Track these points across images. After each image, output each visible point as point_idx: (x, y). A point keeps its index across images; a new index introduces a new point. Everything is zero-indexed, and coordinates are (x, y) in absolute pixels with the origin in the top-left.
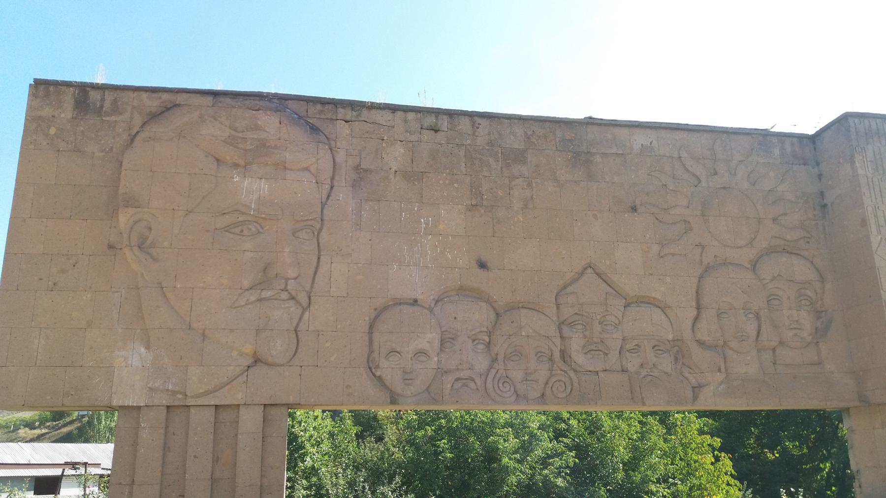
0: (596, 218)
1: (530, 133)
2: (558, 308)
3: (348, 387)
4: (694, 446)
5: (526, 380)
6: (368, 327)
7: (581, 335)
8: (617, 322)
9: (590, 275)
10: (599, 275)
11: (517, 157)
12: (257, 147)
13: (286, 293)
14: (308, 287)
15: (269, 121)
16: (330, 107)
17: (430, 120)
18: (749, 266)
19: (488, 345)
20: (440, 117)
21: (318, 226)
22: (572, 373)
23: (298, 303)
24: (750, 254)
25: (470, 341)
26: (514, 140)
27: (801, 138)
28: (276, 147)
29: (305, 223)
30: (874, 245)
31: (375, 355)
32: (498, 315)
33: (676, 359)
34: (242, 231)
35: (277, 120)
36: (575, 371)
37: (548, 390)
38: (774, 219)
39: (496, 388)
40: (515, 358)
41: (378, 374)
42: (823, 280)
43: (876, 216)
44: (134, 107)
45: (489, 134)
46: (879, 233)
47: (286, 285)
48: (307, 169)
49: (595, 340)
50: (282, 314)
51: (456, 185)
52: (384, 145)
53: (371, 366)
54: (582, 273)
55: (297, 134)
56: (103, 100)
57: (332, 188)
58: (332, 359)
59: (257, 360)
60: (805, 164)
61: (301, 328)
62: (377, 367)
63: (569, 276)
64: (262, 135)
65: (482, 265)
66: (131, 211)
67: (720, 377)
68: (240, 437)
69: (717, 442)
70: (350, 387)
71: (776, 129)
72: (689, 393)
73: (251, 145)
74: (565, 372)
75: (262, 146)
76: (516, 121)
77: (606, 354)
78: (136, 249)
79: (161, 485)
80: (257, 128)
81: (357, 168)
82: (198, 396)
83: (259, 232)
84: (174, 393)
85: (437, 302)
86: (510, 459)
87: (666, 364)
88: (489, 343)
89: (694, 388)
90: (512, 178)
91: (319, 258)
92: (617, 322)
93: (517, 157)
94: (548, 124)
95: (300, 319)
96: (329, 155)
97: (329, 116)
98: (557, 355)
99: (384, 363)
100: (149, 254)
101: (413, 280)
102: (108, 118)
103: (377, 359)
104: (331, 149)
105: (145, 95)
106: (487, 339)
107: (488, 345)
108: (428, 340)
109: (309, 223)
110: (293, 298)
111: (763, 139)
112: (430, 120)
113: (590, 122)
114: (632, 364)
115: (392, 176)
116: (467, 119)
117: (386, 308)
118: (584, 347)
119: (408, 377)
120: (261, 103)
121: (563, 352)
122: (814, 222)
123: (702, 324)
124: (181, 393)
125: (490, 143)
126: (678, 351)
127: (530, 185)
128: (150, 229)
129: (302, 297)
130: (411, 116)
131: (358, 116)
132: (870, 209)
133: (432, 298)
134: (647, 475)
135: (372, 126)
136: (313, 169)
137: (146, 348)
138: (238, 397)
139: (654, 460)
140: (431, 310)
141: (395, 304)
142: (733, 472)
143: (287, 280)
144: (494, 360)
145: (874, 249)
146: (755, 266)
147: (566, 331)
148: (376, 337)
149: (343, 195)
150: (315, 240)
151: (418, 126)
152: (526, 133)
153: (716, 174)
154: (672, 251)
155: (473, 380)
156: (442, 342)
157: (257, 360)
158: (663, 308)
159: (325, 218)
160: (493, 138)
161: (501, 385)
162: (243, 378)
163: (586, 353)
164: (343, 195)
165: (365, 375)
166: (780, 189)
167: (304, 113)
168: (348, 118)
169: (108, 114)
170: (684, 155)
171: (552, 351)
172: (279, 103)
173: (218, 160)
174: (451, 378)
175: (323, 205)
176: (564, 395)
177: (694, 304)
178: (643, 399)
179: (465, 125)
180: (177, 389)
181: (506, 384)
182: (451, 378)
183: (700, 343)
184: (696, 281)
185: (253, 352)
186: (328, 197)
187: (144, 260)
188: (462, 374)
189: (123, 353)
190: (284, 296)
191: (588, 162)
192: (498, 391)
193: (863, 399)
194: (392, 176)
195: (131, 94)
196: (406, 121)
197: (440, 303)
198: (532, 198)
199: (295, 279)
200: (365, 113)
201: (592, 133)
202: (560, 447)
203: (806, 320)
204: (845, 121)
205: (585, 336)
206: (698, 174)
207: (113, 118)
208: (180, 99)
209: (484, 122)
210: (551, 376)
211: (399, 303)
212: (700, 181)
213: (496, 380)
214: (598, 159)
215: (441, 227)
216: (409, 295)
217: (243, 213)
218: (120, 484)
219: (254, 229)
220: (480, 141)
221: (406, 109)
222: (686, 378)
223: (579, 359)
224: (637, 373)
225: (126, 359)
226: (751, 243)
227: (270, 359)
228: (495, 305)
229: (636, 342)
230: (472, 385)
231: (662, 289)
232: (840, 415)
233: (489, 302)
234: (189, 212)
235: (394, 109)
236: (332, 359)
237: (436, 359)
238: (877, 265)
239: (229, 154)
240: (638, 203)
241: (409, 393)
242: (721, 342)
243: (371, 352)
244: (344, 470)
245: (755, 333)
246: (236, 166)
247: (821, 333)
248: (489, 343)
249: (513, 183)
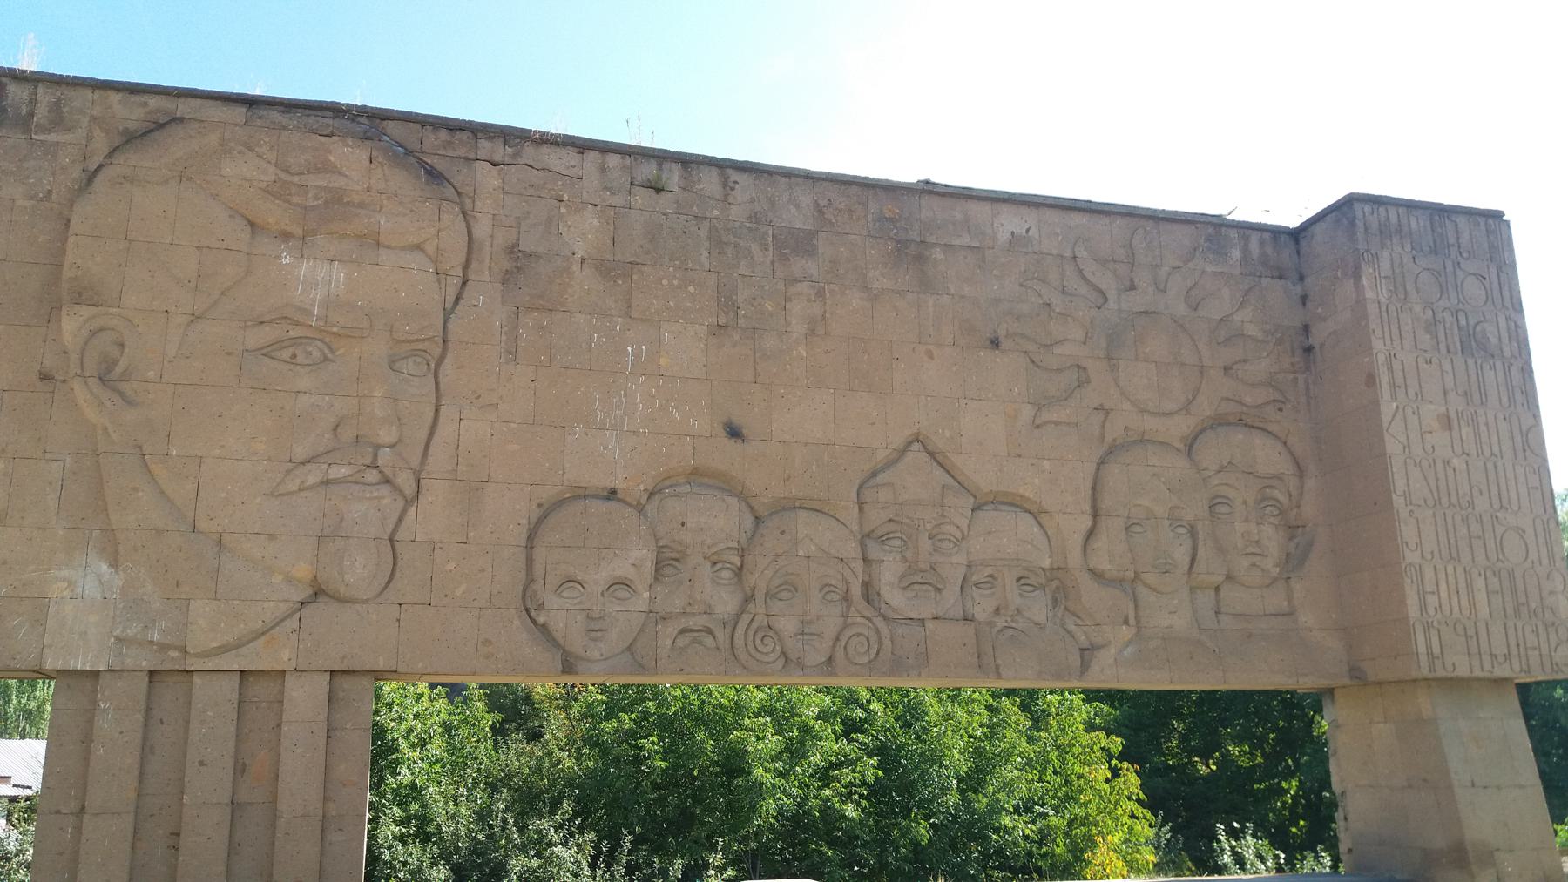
0: (931, 357)
1: (823, 203)
2: (861, 510)
3: (487, 642)
4: (1077, 750)
5: (803, 634)
6: (525, 536)
7: (898, 557)
8: (959, 535)
9: (916, 455)
10: (931, 454)
11: (802, 243)
12: (326, 202)
13: (375, 472)
14: (415, 463)
15: (351, 159)
16: (465, 136)
17: (648, 170)
18: (1181, 446)
19: (739, 571)
20: (667, 165)
21: (437, 352)
22: (880, 622)
23: (397, 489)
24: (1180, 427)
25: (708, 565)
26: (797, 216)
27: (1276, 233)
28: (361, 205)
29: (414, 346)
30: (1386, 419)
31: (538, 586)
32: (758, 520)
33: (1055, 601)
34: (294, 356)
35: (365, 156)
36: (885, 618)
37: (840, 652)
38: (1226, 369)
39: (751, 647)
40: (784, 595)
41: (541, 620)
42: (1301, 473)
43: (1390, 369)
44: (94, 119)
45: (753, 200)
46: (1394, 397)
47: (375, 456)
48: (418, 247)
49: (922, 565)
50: (367, 510)
51: (691, 289)
52: (563, 210)
53: (529, 607)
54: (903, 452)
55: (401, 181)
56: (33, 101)
57: (464, 283)
58: (458, 592)
59: (319, 592)
60: (1280, 278)
61: (402, 535)
62: (541, 607)
63: (882, 455)
64: (337, 182)
65: (734, 432)
66: (86, 311)
67: (1126, 632)
68: (285, 728)
69: (1116, 744)
70: (490, 642)
71: (1237, 216)
72: (1075, 660)
73: (316, 198)
74: (869, 619)
75: (336, 199)
76: (800, 181)
77: (939, 590)
78: (93, 382)
79: (136, 813)
80: (326, 168)
81: (512, 250)
82: (208, 654)
83: (326, 359)
84: (164, 647)
85: (651, 494)
86: (766, 770)
87: (1038, 609)
88: (741, 568)
89: (1082, 650)
90: (791, 281)
91: (437, 411)
92: (959, 535)
93: (802, 243)
94: (854, 190)
95: (400, 519)
96: (460, 224)
97: (462, 152)
98: (856, 590)
99: (552, 602)
100: (121, 394)
101: (610, 454)
102: (42, 137)
103: (540, 594)
104: (464, 213)
105: (115, 97)
106: (737, 561)
107: (739, 571)
108: (635, 559)
109: (421, 346)
110: (388, 481)
111: (1213, 231)
112: (648, 170)
113: (927, 189)
114: (982, 608)
115: (575, 268)
116: (715, 172)
117: (559, 503)
118: (903, 576)
119: (595, 627)
120: (336, 123)
121: (866, 585)
122: (1291, 376)
123: (1100, 543)
124: (176, 648)
125: (754, 217)
126: (1057, 587)
127: (820, 294)
128: (122, 345)
129: (405, 480)
130: (613, 160)
131: (517, 154)
132: (1381, 358)
133: (642, 487)
134: (998, 800)
135: (540, 174)
136: (430, 249)
137: (111, 565)
138: (284, 658)
139: (1010, 773)
140: (640, 509)
141: (576, 497)
142: (1142, 796)
143: (377, 447)
144: (748, 599)
145: (1385, 425)
146: (1191, 446)
147: (874, 551)
148: (540, 553)
149: (484, 297)
150: (431, 377)
151: (626, 180)
152: (816, 203)
153: (1133, 288)
154: (1055, 417)
155: (710, 632)
156: (659, 565)
157: (319, 592)
159: (450, 337)
160: (758, 208)
161: (758, 642)
162: (292, 623)
163: (904, 589)
164: (484, 297)
165: (517, 622)
166: (1238, 318)
167: (414, 145)
168: (497, 159)
169: (43, 129)
170: (1082, 253)
171: (847, 583)
172: (368, 124)
173: (252, 224)
174: (672, 629)
176: (866, 659)
177: (1088, 508)
178: (997, 667)
179: (709, 182)
180: (168, 640)
181: (767, 640)
182: (672, 629)
183: (1096, 574)
184: (1093, 467)
185: (310, 576)
186: (457, 299)
187: (108, 404)
188: (691, 623)
189: (65, 573)
190: (372, 476)
191: (920, 259)
192: (753, 652)
193: (1356, 673)
194: (575, 268)
195: (88, 93)
196: (603, 170)
197: (657, 497)
198: (823, 316)
199: (392, 446)
200: (529, 152)
201: (930, 209)
202: (851, 750)
203: (1272, 540)
204: (1347, 209)
205: (904, 559)
206: (1103, 287)
207: (52, 137)
208: (183, 108)
209: (744, 179)
210: (845, 626)
211: (582, 494)
212: (1106, 300)
213: (751, 633)
214: (938, 254)
215: (663, 361)
216: (601, 481)
217: (297, 324)
218: (58, 812)
219: (316, 353)
220: (734, 212)
221: (604, 148)
222: (1069, 632)
223: (894, 597)
224: (991, 624)
225: (71, 584)
226: (1186, 408)
227: (342, 590)
228: (754, 502)
229: (989, 571)
230: (709, 641)
231: (1037, 481)
232: (1317, 701)
233: (743, 496)
234: (195, 318)
235: (582, 146)
236: (458, 592)
237: (646, 595)
238: (1389, 449)
239: (274, 214)
240: (1002, 333)
241: (596, 655)
242: (1131, 574)
243: (530, 580)
244: (469, 790)
245: (1187, 559)
246: (286, 236)
247: (1294, 562)
248: (741, 568)
249: (792, 290)
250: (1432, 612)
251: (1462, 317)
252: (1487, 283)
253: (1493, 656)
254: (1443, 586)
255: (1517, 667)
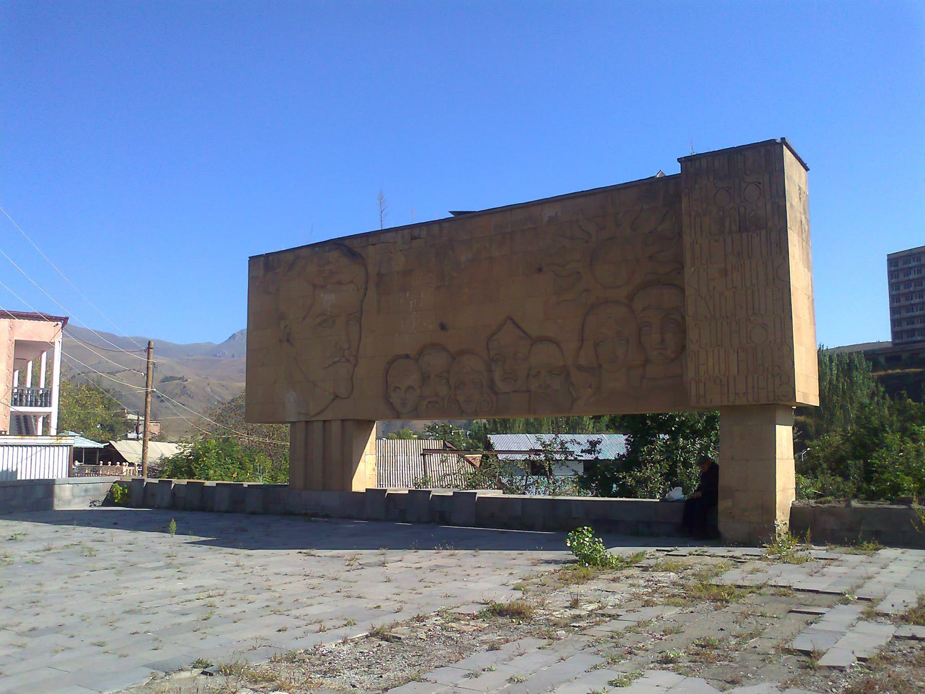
15: (334, 255)
36: (496, 393)
48: (352, 282)
59: (337, 397)
81: (379, 274)
107: (448, 380)
130: (406, 232)
155: (437, 402)
158: (557, 344)
175: (362, 301)
183: (580, 368)
209: (446, 225)
211: (398, 357)
223: (500, 385)
234: (304, 318)
246: (322, 287)
250: (702, 374)
251: (742, 209)
252: (761, 186)
253: (737, 394)
254: (711, 362)
255: (750, 399)
